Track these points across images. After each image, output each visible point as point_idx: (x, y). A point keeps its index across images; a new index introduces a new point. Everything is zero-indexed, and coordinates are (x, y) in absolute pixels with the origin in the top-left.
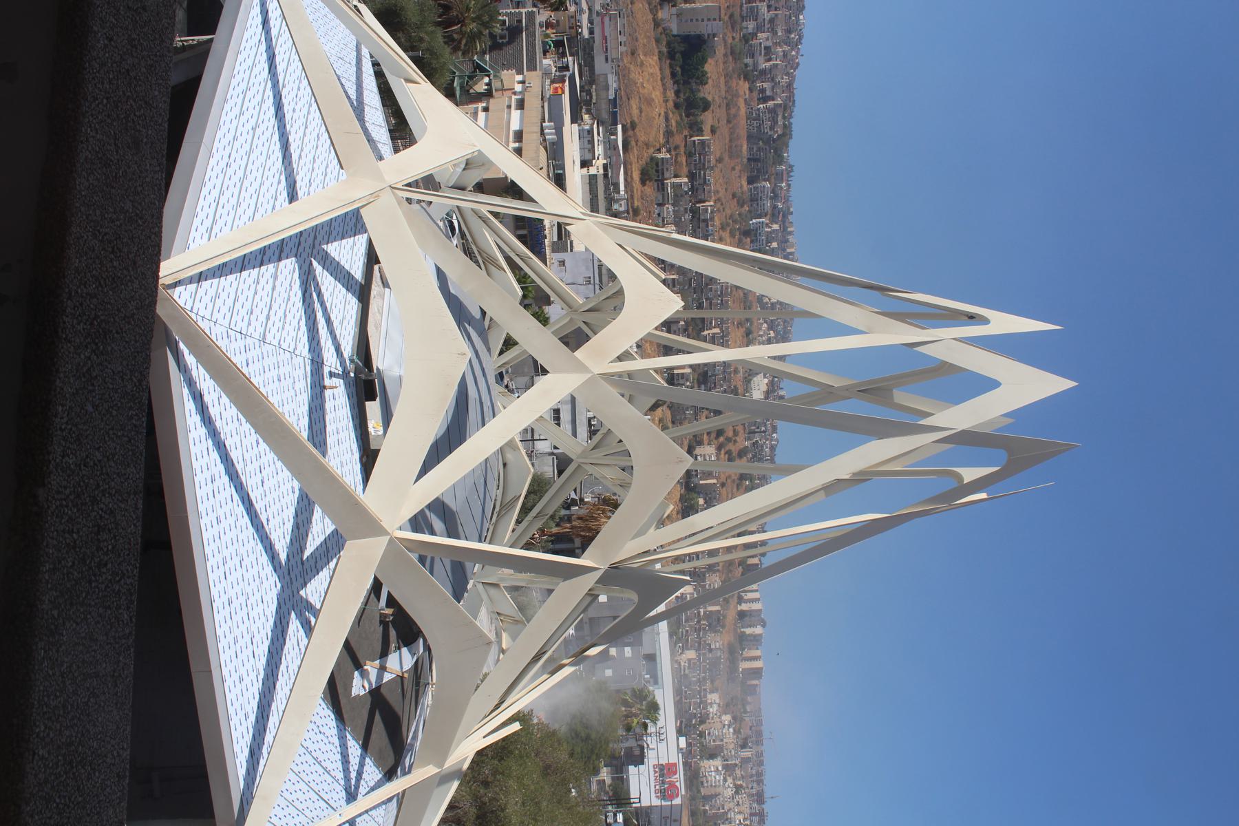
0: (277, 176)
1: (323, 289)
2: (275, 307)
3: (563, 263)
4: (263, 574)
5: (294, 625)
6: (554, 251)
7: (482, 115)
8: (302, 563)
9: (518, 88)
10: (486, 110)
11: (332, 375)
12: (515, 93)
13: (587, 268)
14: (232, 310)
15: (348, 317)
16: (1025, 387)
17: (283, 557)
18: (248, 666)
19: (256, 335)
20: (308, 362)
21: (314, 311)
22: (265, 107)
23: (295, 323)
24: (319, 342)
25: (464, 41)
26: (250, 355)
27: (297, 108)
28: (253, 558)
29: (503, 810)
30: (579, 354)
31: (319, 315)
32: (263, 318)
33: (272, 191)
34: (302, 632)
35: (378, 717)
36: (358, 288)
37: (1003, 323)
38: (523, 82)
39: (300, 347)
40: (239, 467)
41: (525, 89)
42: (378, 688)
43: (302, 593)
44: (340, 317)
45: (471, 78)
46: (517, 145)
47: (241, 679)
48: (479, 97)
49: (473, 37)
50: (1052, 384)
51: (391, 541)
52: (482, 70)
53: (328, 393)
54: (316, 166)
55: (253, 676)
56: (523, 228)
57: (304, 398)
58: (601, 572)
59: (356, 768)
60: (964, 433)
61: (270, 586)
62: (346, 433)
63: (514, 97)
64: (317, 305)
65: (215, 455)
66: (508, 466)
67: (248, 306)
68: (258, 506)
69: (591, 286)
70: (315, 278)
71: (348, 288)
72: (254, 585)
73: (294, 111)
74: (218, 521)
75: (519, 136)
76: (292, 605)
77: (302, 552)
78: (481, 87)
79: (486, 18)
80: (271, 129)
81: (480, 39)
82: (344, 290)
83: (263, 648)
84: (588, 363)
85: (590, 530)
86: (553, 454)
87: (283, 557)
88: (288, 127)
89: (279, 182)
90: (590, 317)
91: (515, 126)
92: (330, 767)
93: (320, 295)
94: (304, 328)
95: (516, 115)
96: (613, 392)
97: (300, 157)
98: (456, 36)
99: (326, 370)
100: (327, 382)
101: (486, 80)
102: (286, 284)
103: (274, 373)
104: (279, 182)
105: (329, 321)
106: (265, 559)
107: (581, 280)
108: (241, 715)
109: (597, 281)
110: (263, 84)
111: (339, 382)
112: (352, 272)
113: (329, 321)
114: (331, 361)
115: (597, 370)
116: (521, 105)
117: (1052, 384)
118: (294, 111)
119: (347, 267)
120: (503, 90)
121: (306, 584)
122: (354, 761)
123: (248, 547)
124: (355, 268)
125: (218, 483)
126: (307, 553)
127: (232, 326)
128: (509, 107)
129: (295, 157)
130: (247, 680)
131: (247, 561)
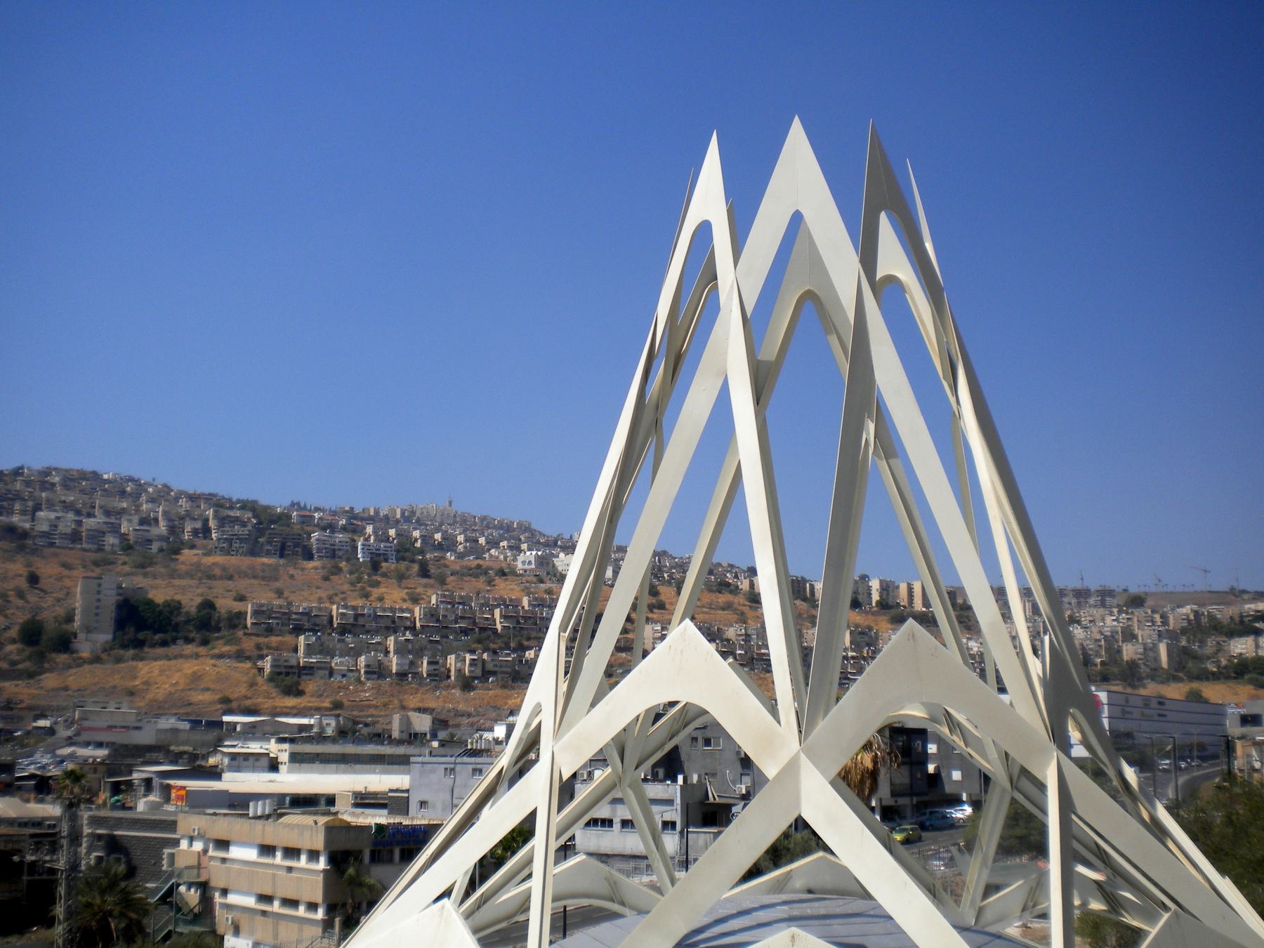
3: (423, 804)
6: (406, 812)
7: (233, 899)
9: (198, 846)
10: (225, 892)
12: (205, 851)
13: (433, 771)
16: (799, 178)
25: (133, 916)
30: (770, 770)
37: (708, 199)
38: (191, 839)
41: (201, 836)
45: (179, 910)
46: (279, 854)
48: (206, 900)
49: (127, 901)
50: (797, 142)
52: (170, 892)
56: (391, 852)
60: (862, 261)
63: (211, 853)
66: (812, 885)
69: (458, 768)
75: (267, 850)
78: (192, 897)
79: (105, 882)
81: (129, 893)
84: (784, 758)
85: (862, 781)
86: (681, 832)
90: (631, 758)
91: (251, 854)
95: (236, 852)
96: (822, 725)
98: (123, 925)
101: (182, 889)
107: (448, 781)
109: (452, 759)
115: (793, 744)
116: (223, 844)
117: (797, 142)
120: (199, 867)
128: (224, 860)
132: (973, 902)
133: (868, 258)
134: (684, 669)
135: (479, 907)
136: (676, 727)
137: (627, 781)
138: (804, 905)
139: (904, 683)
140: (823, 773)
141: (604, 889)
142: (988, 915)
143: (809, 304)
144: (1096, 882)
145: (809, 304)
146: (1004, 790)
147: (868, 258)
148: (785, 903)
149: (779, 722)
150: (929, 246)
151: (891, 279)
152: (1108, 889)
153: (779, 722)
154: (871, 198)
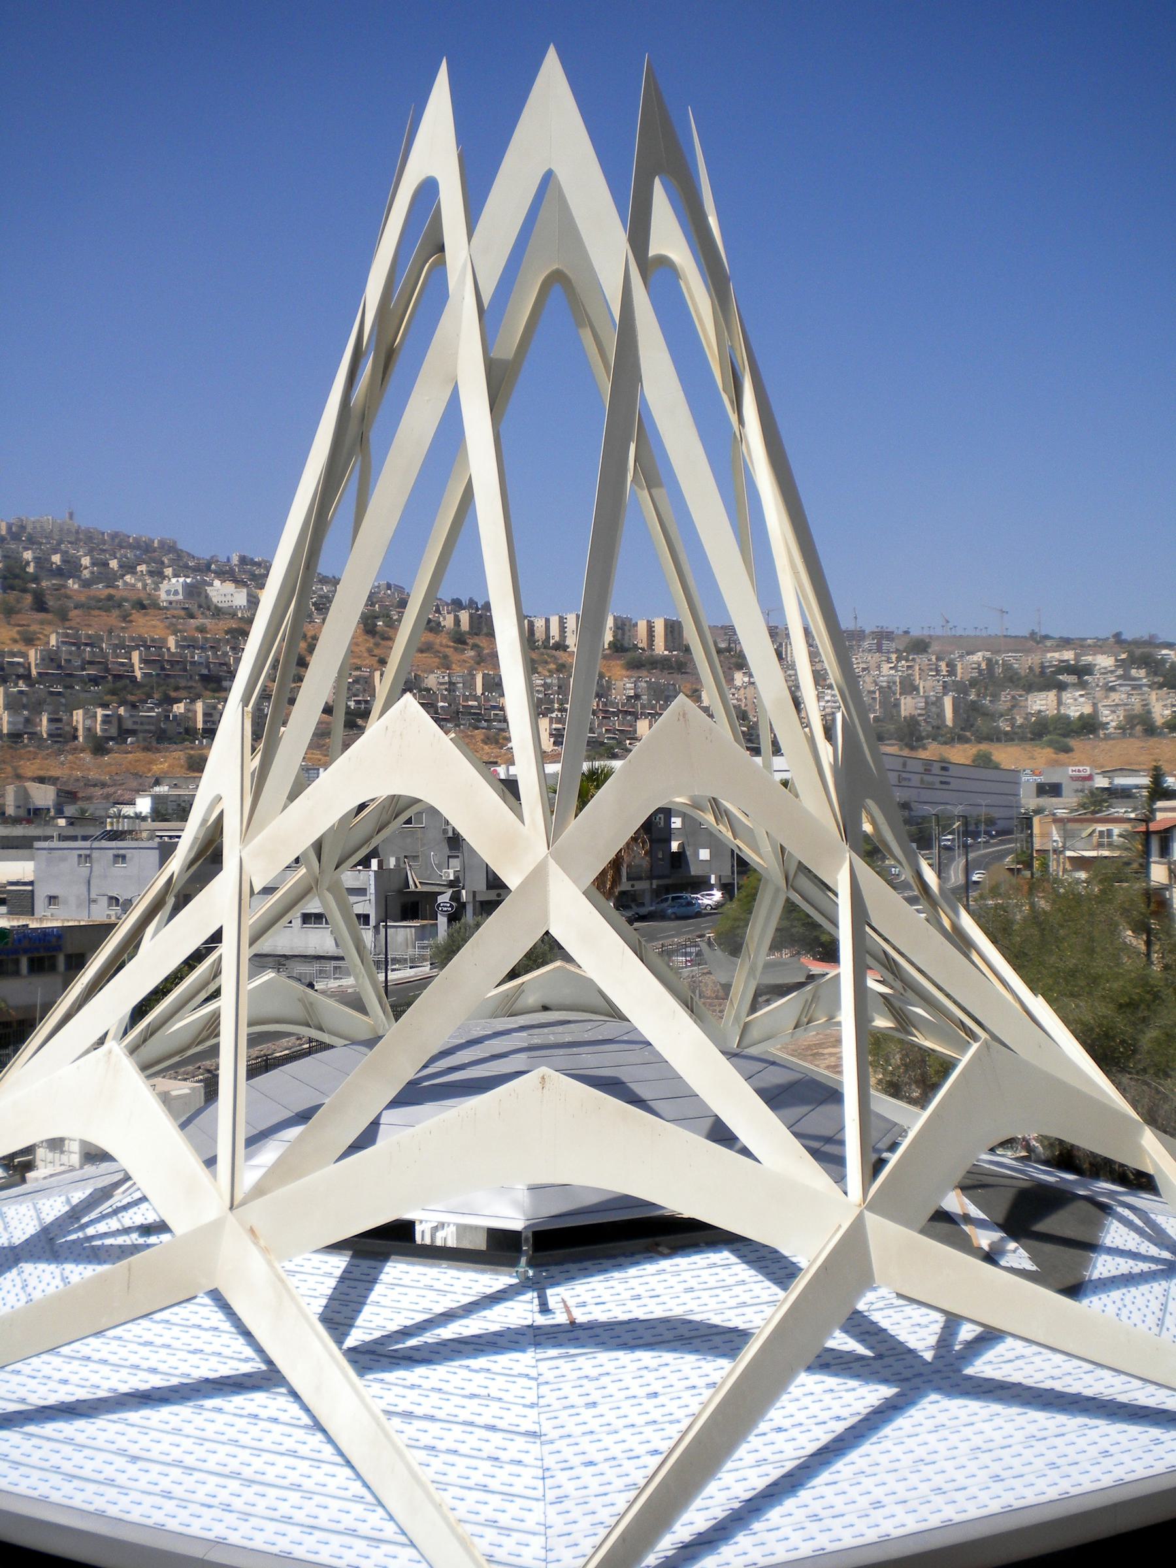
0: (207, 1414)
1: (393, 1327)
2: (464, 1415)
3: (52, 899)
4: (929, 1424)
5: (984, 1367)
6: (31, 911)
8: (879, 1357)
11: (544, 1309)
13: (63, 859)
14: (510, 1496)
15: (425, 1281)
16: (553, 128)
17: (886, 1391)
18: (1082, 1443)
19: (535, 1448)
20: (542, 1354)
21: (444, 1343)
22: (80, 1438)
23: (480, 1378)
24: (495, 1334)
26: (576, 1461)
27: (57, 1376)
28: (911, 1443)
29: (1092, 1029)
30: (512, 880)
31: (448, 1332)
32: (497, 1438)
33: (242, 1423)
34: (990, 1355)
35: (1040, 1227)
36: (365, 1264)
37: (435, 148)
39: (519, 1368)
40: (775, 1474)
42: (1003, 1227)
43: (928, 1356)
44: (432, 1295)
47: (1106, 1453)
51: (871, 1207)
53: (581, 1317)
54: (158, 1341)
55: (1093, 1435)
56: (17, 962)
57: (608, 1360)
58: (854, 855)
59: (1131, 1262)
61: (935, 1410)
62: (633, 1283)
64: (429, 1337)
65: (774, 1515)
66: (547, 1001)
67: (486, 1466)
68: (823, 1437)
69: (95, 854)
70: (376, 1342)
71: (371, 1281)
72: (954, 1439)
73: (65, 1382)
74: (877, 1505)
76: (947, 1370)
77: (862, 1358)
80: (120, 1427)
82: (378, 1289)
83: (1040, 1417)
86: (376, 928)
87: (886, 1391)
88: (102, 1394)
89: (220, 1410)
92: (1155, 1306)
93: (406, 1333)
94: (481, 1362)
97: (153, 1371)
99: (541, 1320)
100: (561, 1318)
102: (413, 1395)
103: (587, 1414)
104: (220, 1410)
105: (448, 1316)
106: (902, 1423)
107: (84, 871)
108: (1159, 1450)
109: (87, 844)
110: (35, 1441)
111: (555, 1295)
112: (338, 1273)
113: (448, 1316)
114: (520, 1312)
118: (65, 1382)
119: (332, 1283)
121: (911, 1351)
122: (1125, 1266)
123: (897, 1451)
124: (326, 1268)
125: (816, 1507)
126: (861, 1350)
127: (538, 1493)
129: (156, 1381)
130: (1104, 1444)
131: (921, 1452)
132: (737, 1018)
133: (639, 234)
134: (405, 754)
135: (145, 1041)
136: (385, 817)
137: (326, 883)
138: (546, 1030)
139: (670, 766)
140: (575, 881)
141: (298, 1012)
142: (755, 1033)
143: (557, 289)
144: (881, 995)
145: (557, 289)
146: (778, 890)
147: (639, 234)
148: (522, 1028)
149: (523, 822)
150: (713, 221)
151: (663, 261)
152: (897, 1004)
153: (523, 822)
154: (643, 159)
